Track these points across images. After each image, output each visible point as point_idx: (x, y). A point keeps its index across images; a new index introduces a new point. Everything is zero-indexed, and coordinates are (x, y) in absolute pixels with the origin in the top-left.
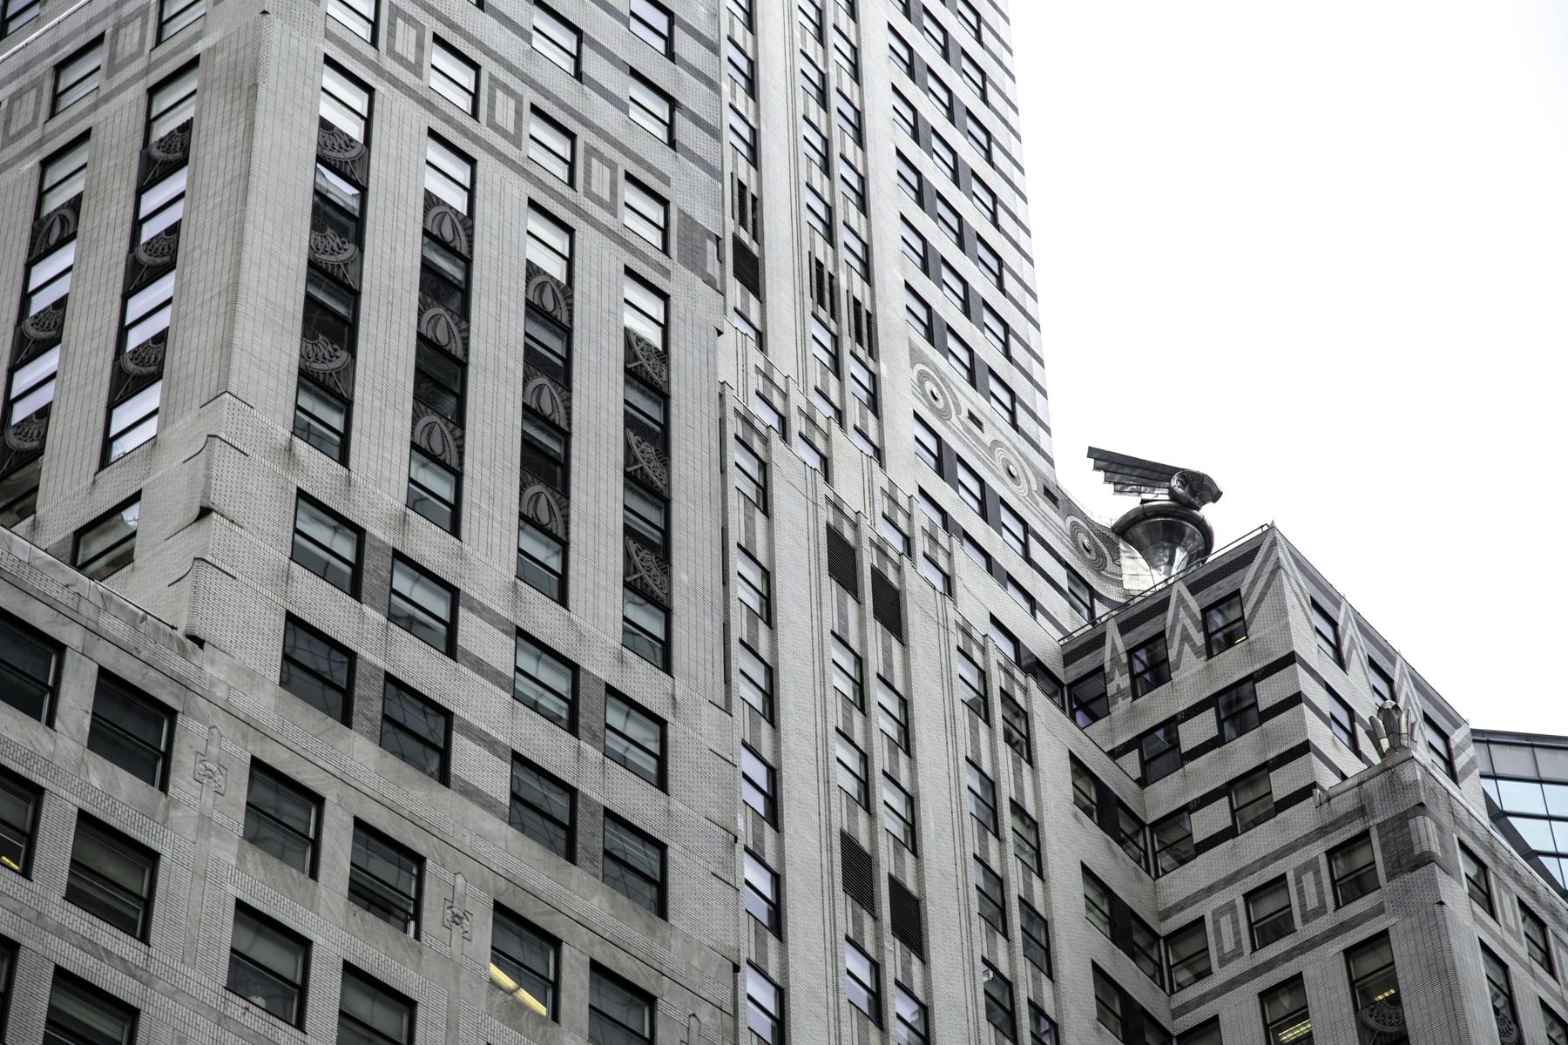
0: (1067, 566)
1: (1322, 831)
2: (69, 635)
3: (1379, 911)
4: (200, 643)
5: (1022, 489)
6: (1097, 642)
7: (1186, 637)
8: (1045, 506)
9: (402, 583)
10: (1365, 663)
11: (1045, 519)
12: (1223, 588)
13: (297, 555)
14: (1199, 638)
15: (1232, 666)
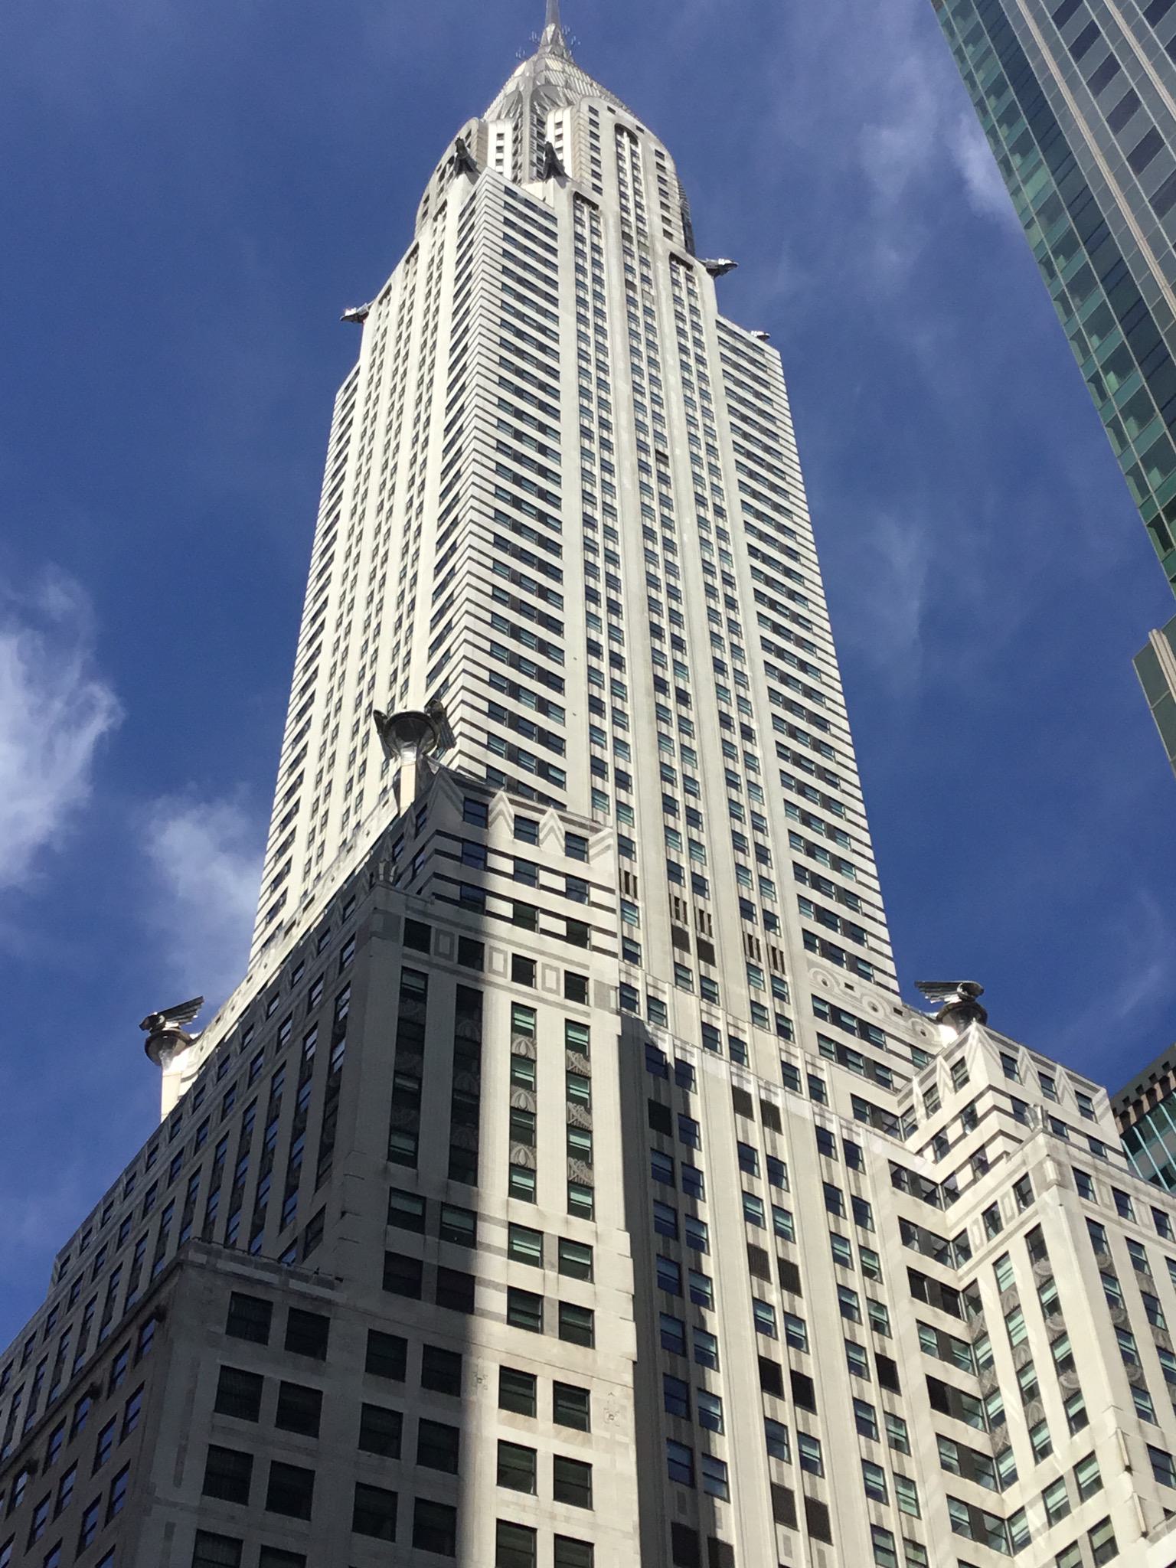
0: (911, 1046)
1: (1010, 1175)
2: (274, 1297)
3: (1036, 1213)
4: (341, 1280)
5: (880, 1014)
6: (911, 1092)
7: (946, 1085)
8: (896, 1018)
9: (450, 1218)
10: (1036, 1076)
11: (897, 1026)
12: (957, 1057)
13: (392, 1220)
14: (951, 1084)
15: (966, 1094)
